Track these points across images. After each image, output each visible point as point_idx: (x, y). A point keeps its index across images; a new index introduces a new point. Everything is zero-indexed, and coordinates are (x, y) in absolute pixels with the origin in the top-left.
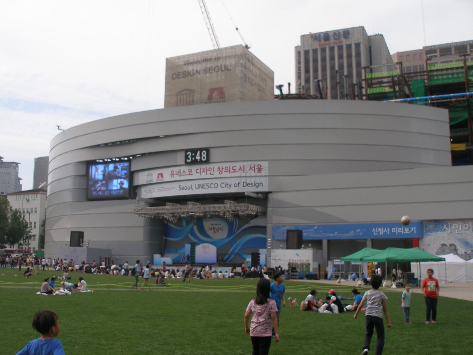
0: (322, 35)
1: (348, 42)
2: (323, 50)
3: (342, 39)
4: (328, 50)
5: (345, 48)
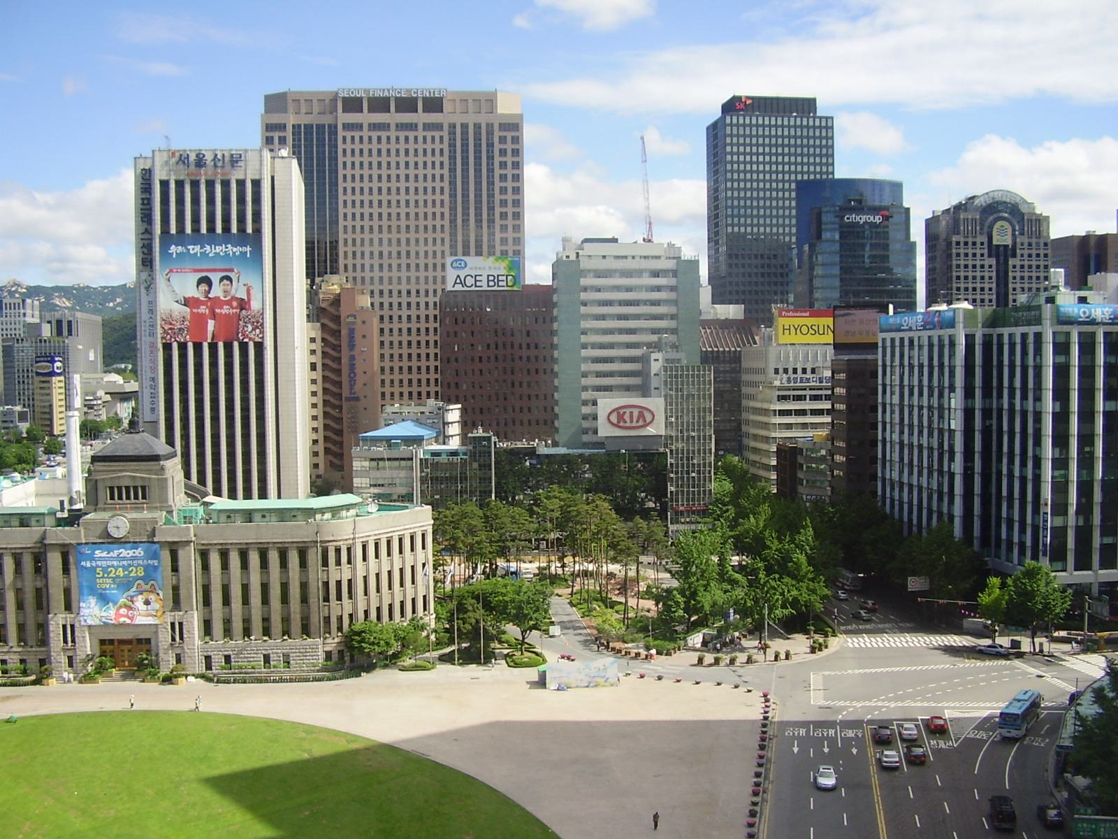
0: (193, 157)
1: (241, 177)
2: (195, 184)
5: (234, 186)
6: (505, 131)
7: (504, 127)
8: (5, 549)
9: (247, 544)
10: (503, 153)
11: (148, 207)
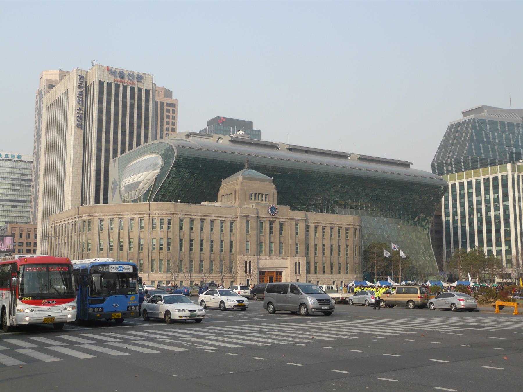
0: (118, 71)
2: (117, 86)
3: (135, 81)
4: (121, 88)
5: (136, 90)
6: (169, 106)
7: (169, 105)
8: (217, 217)
9: (326, 224)
10: (168, 117)
11: (82, 96)
